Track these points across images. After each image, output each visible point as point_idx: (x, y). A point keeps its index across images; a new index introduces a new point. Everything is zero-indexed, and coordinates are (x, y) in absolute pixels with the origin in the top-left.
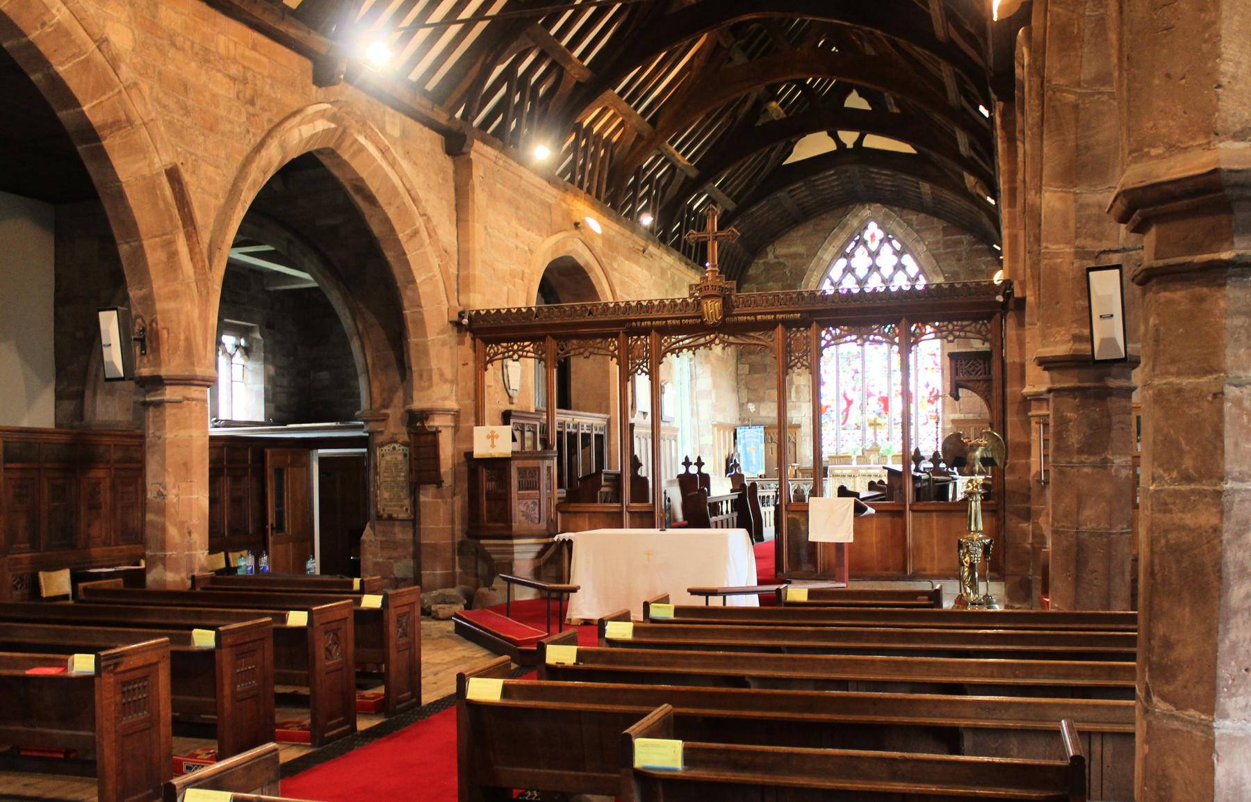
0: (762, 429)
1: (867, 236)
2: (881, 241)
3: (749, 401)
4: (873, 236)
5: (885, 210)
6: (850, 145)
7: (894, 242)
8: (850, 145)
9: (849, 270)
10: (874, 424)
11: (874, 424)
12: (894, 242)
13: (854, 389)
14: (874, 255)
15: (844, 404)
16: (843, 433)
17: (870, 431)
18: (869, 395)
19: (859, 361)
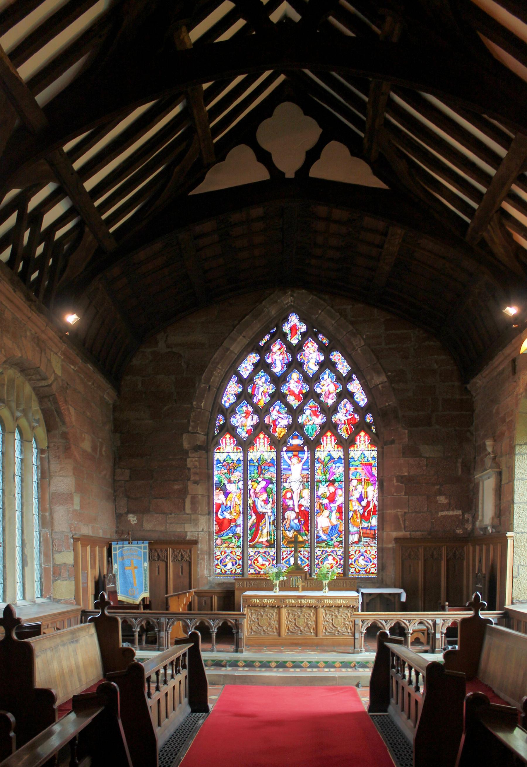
0: (146, 544)
1: (286, 328)
2: (303, 334)
3: (129, 512)
4: (294, 329)
5: (311, 297)
6: (290, 174)
7: (320, 336)
8: (290, 174)
9: (262, 366)
10: (295, 542)
11: (295, 542)
12: (320, 336)
13: (266, 502)
14: (295, 350)
15: (253, 518)
16: (251, 552)
17: (286, 551)
18: (287, 508)
19: (273, 469)
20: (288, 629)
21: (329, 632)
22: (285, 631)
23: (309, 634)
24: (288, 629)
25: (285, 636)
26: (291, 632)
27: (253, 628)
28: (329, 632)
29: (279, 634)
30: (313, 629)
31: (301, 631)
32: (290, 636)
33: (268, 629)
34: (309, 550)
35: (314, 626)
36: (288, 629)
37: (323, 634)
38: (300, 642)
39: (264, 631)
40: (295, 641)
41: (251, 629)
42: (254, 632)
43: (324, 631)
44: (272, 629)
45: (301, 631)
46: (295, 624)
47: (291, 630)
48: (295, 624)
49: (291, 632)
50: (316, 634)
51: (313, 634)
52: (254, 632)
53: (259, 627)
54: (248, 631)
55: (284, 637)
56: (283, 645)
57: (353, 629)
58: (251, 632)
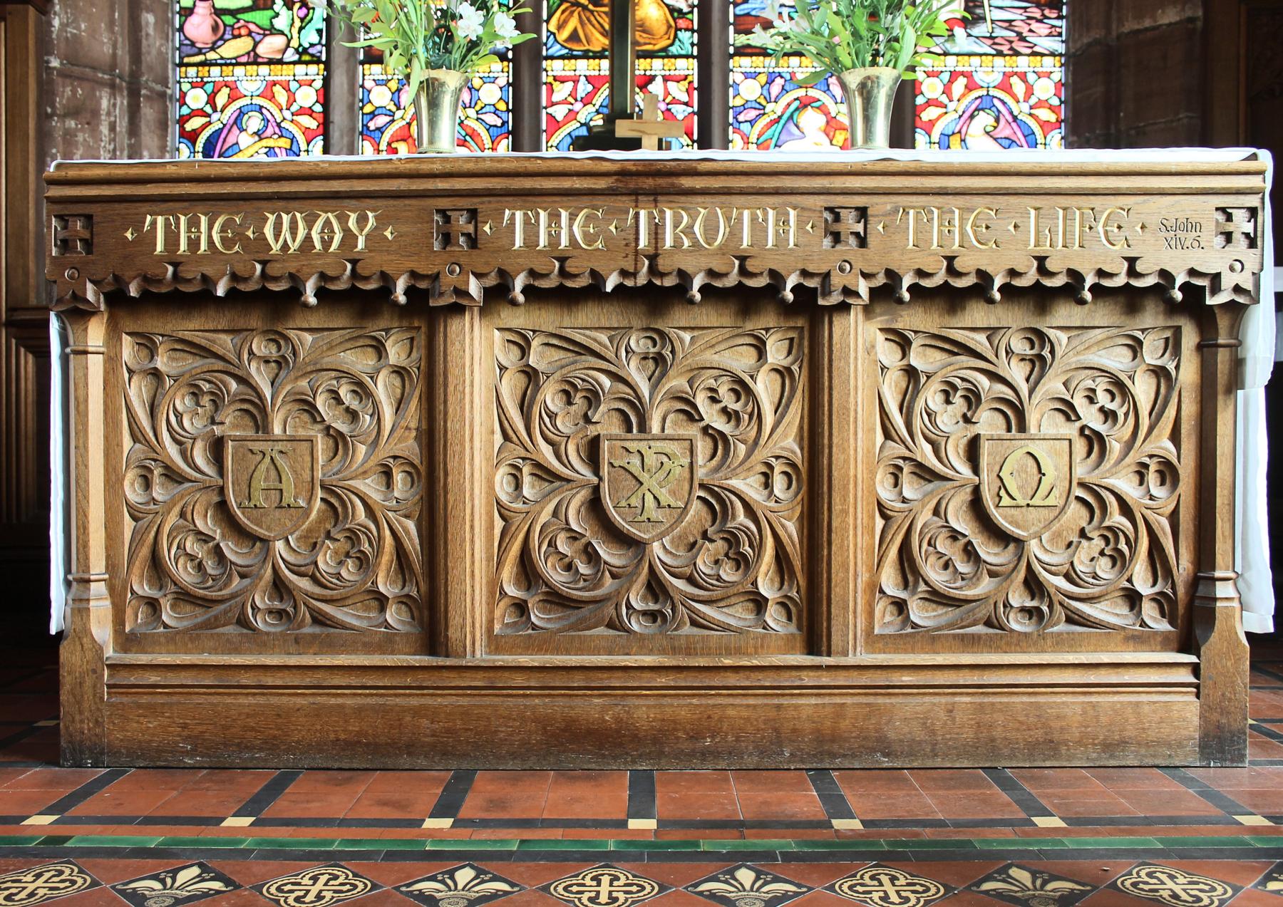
20: (525, 560)
21: (937, 597)
22: (495, 590)
23: (737, 615)
24: (525, 560)
25: (495, 644)
26: (556, 599)
27: (168, 554)
28: (937, 597)
29: (432, 624)
30: (782, 558)
31: (656, 588)
32: (542, 642)
33: (325, 562)
34: (689, 67)
35: (791, 529)
36: (528, 572)
37: (885, 619)
38: (644, 712)
39: (279, 587)
40: (593, 708)
41: (156, 566)
42: (184, 597)
43: (889, 580)
44: (363, 562)
45: (656, 588)
46: (595, 505)
47: (556, 576)
48: (595, 505)
49: (556, 599)
50: (815, 636)
51: (773, 616)
52: (184, 597)
53: (231, 549)
54: (117, 593)
55: (481, 655)
56: (457, 755)
57: (1183, 566)
58: (153, 604)
